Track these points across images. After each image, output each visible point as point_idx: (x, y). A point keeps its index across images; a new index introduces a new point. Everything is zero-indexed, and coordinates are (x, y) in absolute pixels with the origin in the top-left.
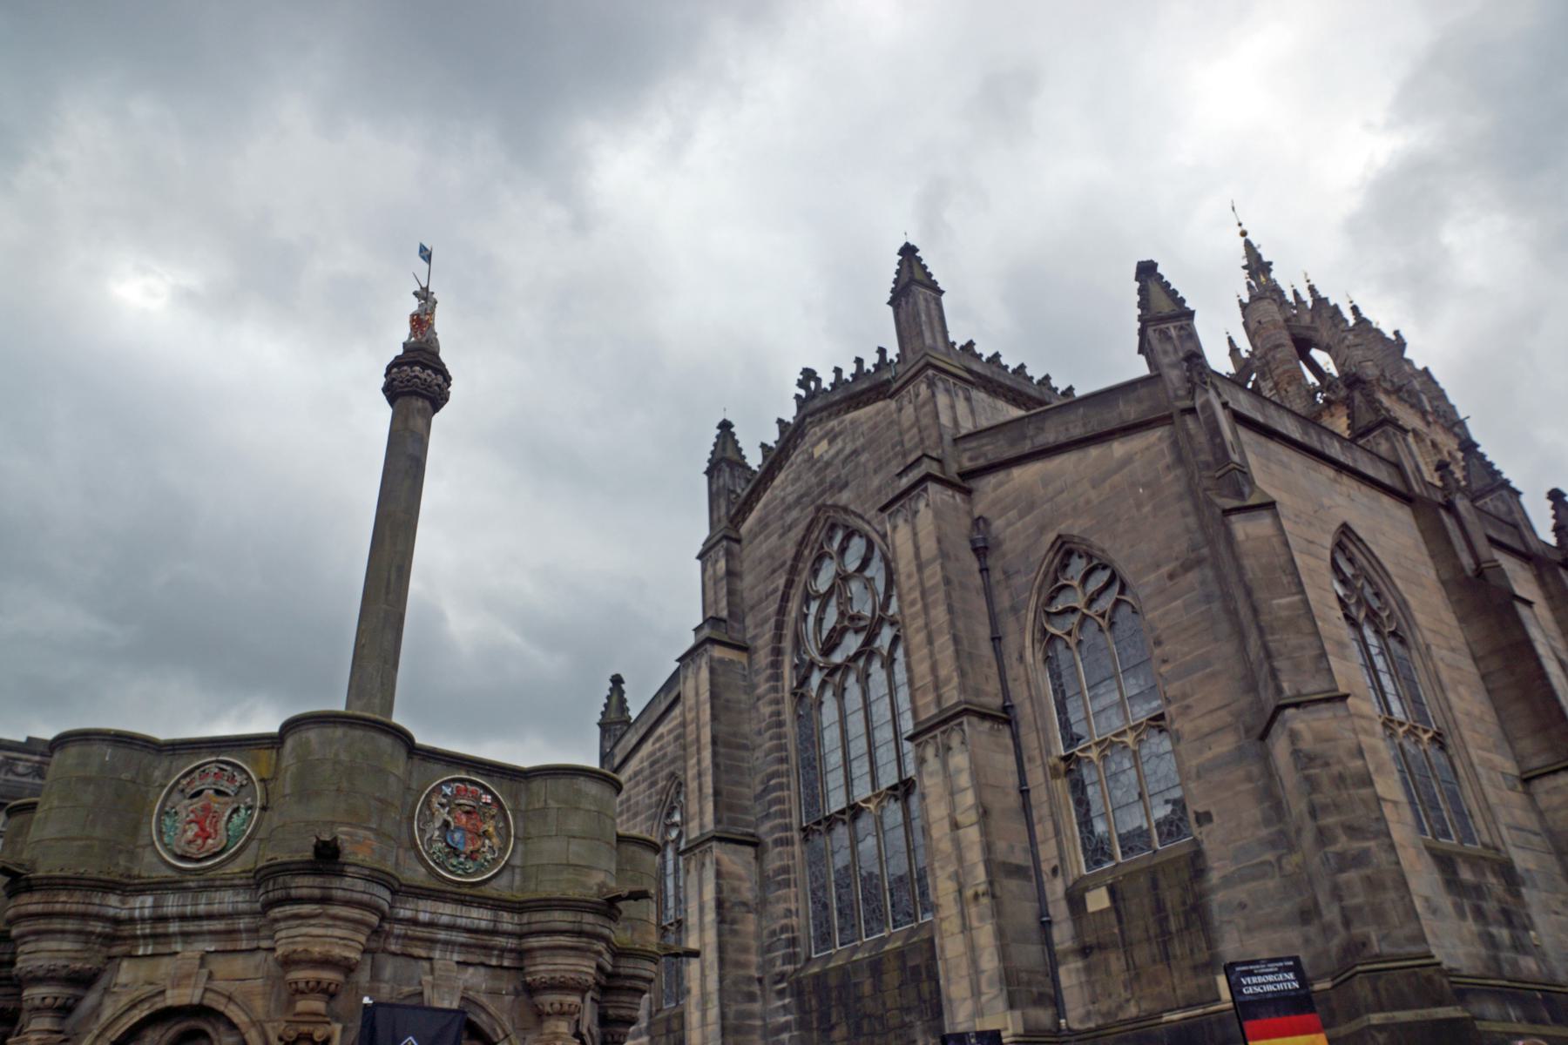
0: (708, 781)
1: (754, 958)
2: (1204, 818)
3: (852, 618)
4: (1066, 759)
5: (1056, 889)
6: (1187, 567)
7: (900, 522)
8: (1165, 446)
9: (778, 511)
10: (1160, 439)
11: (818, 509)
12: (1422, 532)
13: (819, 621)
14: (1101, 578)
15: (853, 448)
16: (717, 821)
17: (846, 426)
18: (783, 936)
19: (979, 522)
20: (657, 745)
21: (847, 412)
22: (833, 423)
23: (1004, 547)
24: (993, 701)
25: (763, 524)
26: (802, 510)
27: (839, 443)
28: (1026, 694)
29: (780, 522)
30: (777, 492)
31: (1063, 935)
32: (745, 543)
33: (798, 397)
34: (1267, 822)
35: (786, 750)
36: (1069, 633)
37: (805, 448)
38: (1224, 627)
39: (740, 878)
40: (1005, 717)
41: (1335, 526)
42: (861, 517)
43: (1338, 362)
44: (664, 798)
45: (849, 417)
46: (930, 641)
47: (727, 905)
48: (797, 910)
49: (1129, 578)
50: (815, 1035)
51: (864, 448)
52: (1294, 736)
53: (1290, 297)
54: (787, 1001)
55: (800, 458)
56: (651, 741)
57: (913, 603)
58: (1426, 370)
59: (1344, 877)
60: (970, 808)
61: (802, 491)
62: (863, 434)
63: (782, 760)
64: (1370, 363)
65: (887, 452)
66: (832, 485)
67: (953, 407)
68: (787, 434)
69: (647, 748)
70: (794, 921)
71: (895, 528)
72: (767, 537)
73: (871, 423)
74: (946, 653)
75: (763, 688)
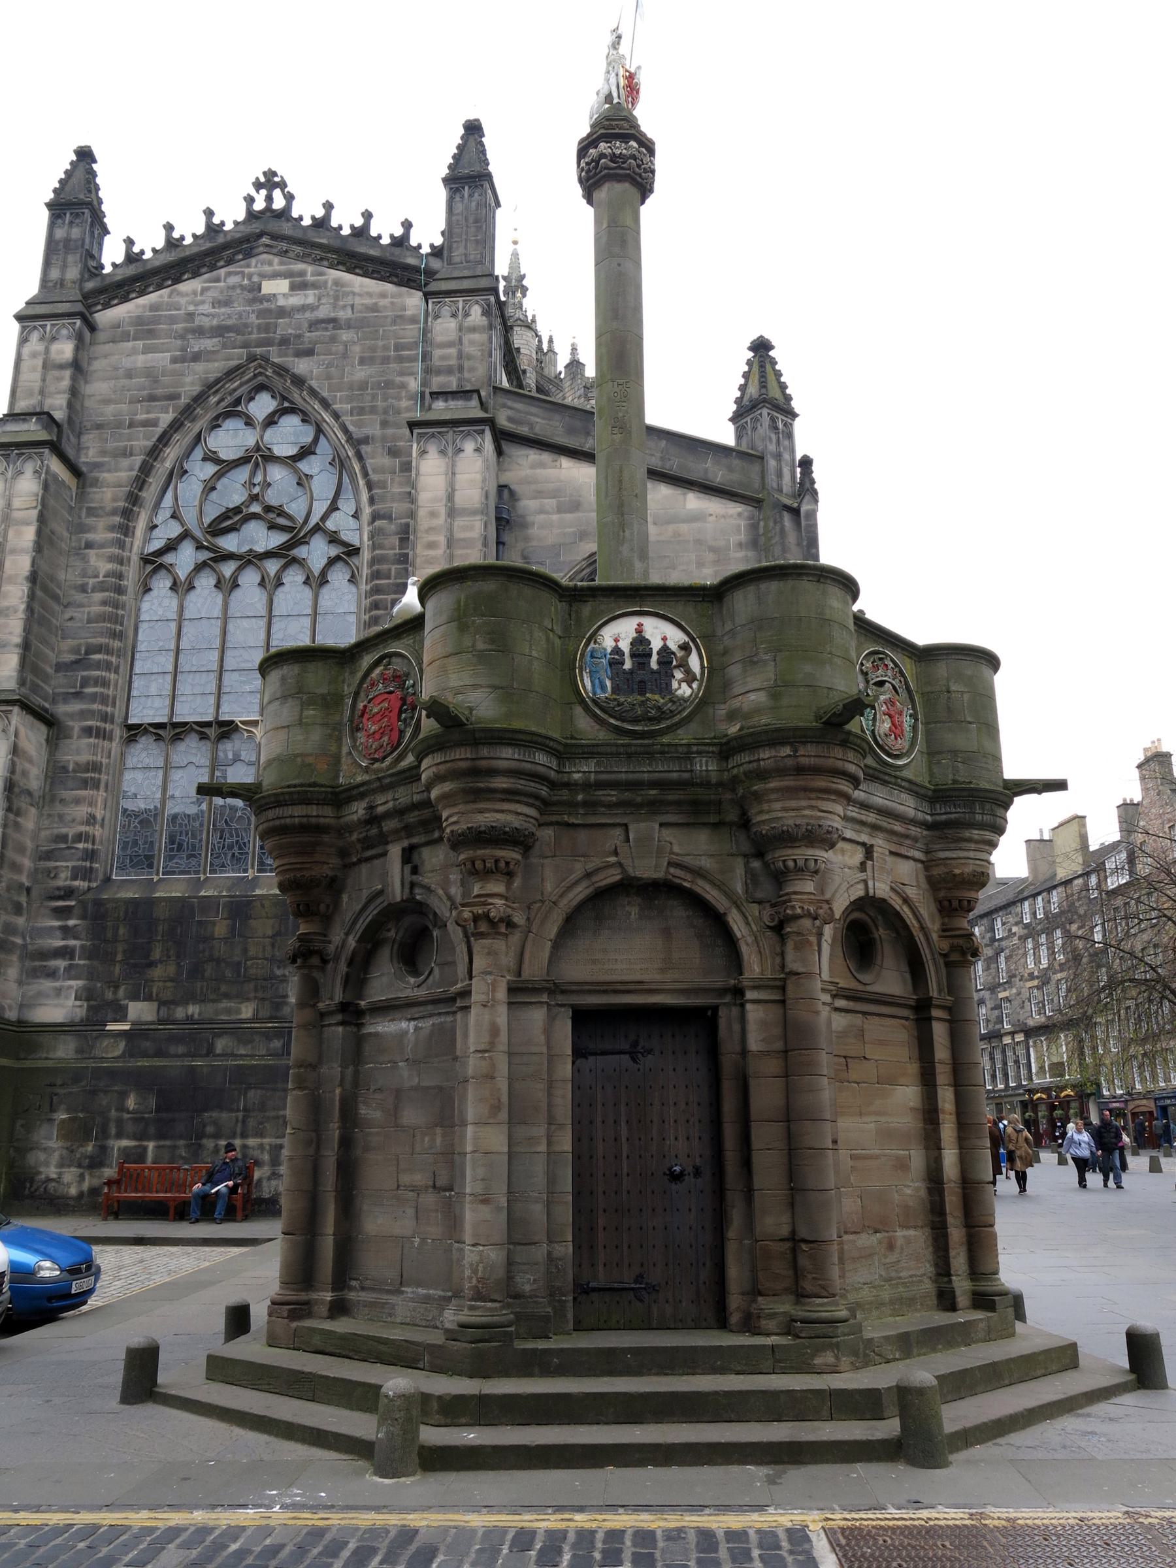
1: (27, 863)
3: (268, 509)
7: (433, 450)
8: (743, 523)
10: (740, 514)
11: (252, 358)
13: (209, 487)
15: (332, 315)
16: (22, 682)
17: (326, 282)
18: (81, 846)
22: (299, 266)
23: (530, 531)
25: (144, 329)
26: (224, 346)
27: (310, 297)
29: (179, 342)
30: (183, 301)
32: (101, 336)
35: (122, 625)
37: (246, 270)
39: (30, 761)
42: (325, 404)
45: (334, 274)
47: (16, 790)
48: (103, 820)
50: (117, 970)
51: (349, 325)
54: (71, 923)
55: (233, 280)
57: (431, 545)
61: (230, 322)
62: (352, 306)
63: (114, 635)
65: (386, 348)
66: (284, 342)
68: (221, 239)
70: (97, 831)
71: (423, 453)
72: (146, 350)
73: (368, 301)
75: (101, 533)
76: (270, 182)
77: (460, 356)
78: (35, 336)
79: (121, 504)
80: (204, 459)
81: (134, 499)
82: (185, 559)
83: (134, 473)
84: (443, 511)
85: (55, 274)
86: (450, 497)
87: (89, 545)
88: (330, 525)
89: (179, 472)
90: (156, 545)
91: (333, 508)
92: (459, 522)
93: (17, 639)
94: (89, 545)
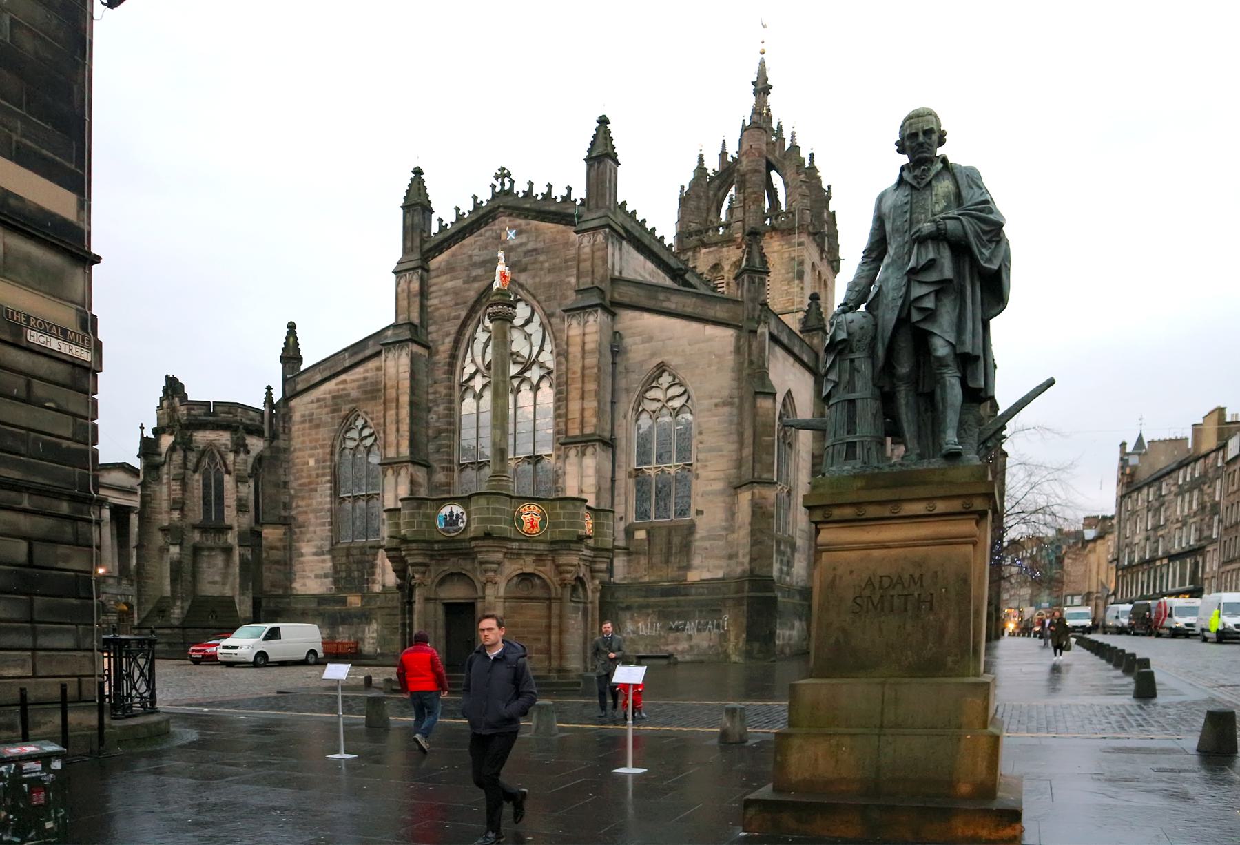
0: (405, 427)
2: (700, 512)
3: (512, 354)
4: (636, 470)
6: (725, 404)
12: (815, 391)
14: (680, 390)
19: (616, 334)
20: (341, 386)
24: (607, 435)
28: (624, 435)
34: (727, 520)
36: (654, 412)
38: (735, 437)
40: (609, 444)
42: (534, 297)
43: (789, 199)
49: (693, 395)
58: (834, 212)
64: (808, 212)
69: (330, 385)
74: (591, 404)
79: (448, 360)
82: (478, 383)
88: (541, 359)
90: (465, 377)
91: (541, 350)
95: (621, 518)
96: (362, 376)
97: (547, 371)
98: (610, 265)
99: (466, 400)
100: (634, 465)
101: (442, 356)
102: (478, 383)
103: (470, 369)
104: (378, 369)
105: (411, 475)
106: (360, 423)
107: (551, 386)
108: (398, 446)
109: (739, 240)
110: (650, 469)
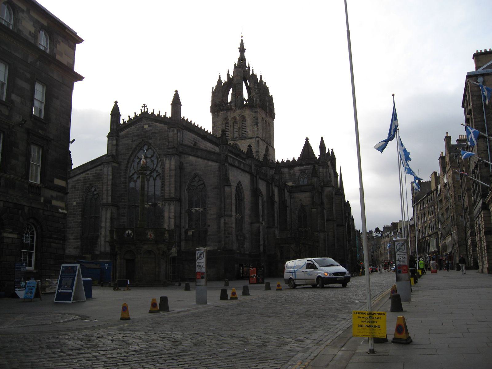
0: (110, 193)
2: (209, 226)
4: (188, 210)
5: (183, 230)
9: (132, 135)
11: (143, 140)
18: (123, 226)
19: (181, 163)
21: (155, 122)
25: (126, 136)
27: (151, 128)
31: (183, 237)
33: (141, 110)
36: (194, 190)
37: (142, 124)
40: (179, 200)
41: (237, 182)
42: (154, 148)
44: (88, 188)
45: (155, 123)
46: (170, 185)
52: (225, 220)
53: (247, 65)
55: (139, 125)
56: (84, 174)
57: (167, 176)
58: (272, 96)
59: (226, 239)
60: (173, 216)
67: (180, 135)
69: (83, 175)
71: (166, 160)
73: (160, 128)
75: (123, 174)
76: (144, 106)
77: (173, 139)
78: (110, 140)
80: (137, 158)
81: (127, 167)
83: (126, 163)
84: (169, 170)
85: (112, 128)
86: (170, 168)
87: (121, 176)
88: (157, 169)
89: (134, 161)
90: (131, 174)
91: (157, 166)
92: (171, 172)
93: (111, 195)
94: (121, 176)
95: (183, 227)
96: (94, 172)
97: (159, 174)
98: (179, 140)
99: (131, 183)
100: (187, 208)
101: (123, 167)
102: (135, 176)
103: (133, 171)
104: (101, 170)
105: (112, 210)
106: (93, 189)
107: (160, 179)
108: (107, 199)
109: (234, 109)
110: (193, 210)
